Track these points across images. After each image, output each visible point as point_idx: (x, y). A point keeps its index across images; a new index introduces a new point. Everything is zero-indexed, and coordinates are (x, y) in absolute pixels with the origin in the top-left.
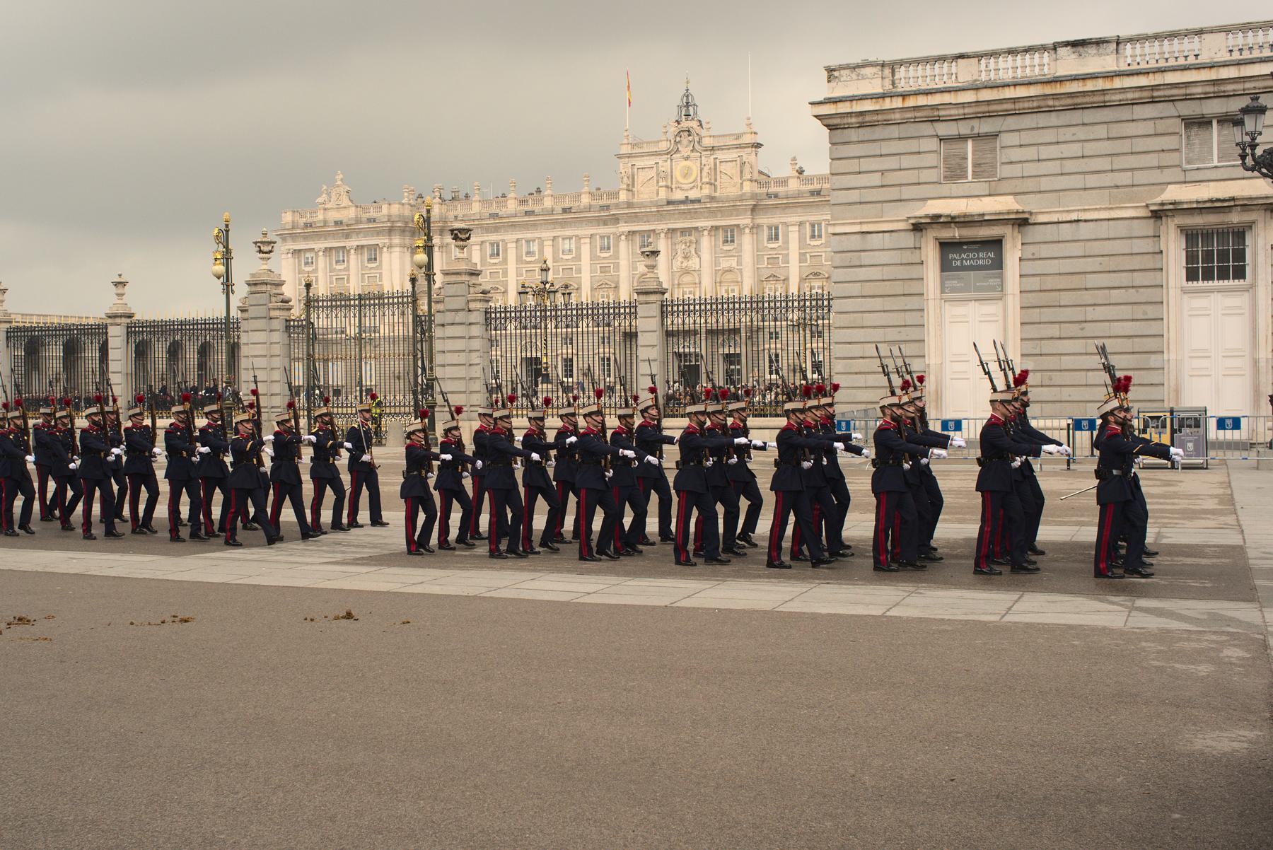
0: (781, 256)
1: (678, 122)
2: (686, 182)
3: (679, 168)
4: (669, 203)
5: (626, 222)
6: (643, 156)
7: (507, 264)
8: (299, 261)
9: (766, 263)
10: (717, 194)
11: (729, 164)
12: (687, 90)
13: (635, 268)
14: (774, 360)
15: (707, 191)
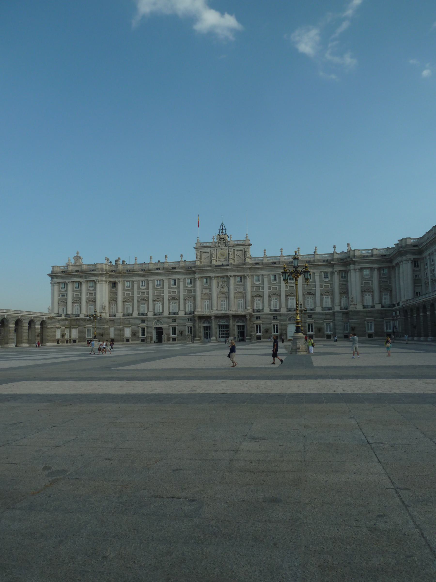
0: (260, 287)
1: (219, 235)
2: (222, 258)
3: (219, 252)
4: (216, 266)
5: (198, 273)
6: (205, 248)
7: (148, 289)
8: (59, 287)
9: (255, 290)
10: (234, 263)
11: (240, 252)
12: (222, 223)
13: (202, 291)
14: (258, 327)
15: (231, 262)
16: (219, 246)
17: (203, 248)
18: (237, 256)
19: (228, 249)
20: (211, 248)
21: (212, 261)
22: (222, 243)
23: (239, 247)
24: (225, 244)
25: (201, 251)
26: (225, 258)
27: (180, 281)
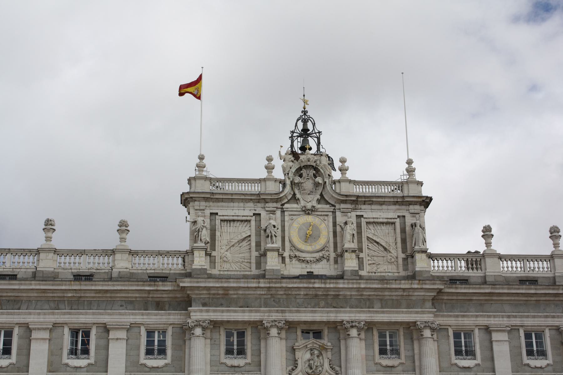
2: (309, 248)
5: (204, 305)
6: (232, 200)
11: (384, 227)
12: (305, 112)
15: (351, 263)
16: (294, 199)
17: (222, 200)
18: (369, 245)
19: (334, 212)
20: (259, 205)
21: (264, 255)
22: (308, 185)
23: (378, 207)
24: (319, 192)
25: (211, 214)
26: (321, 250)
27: (110, 337)
